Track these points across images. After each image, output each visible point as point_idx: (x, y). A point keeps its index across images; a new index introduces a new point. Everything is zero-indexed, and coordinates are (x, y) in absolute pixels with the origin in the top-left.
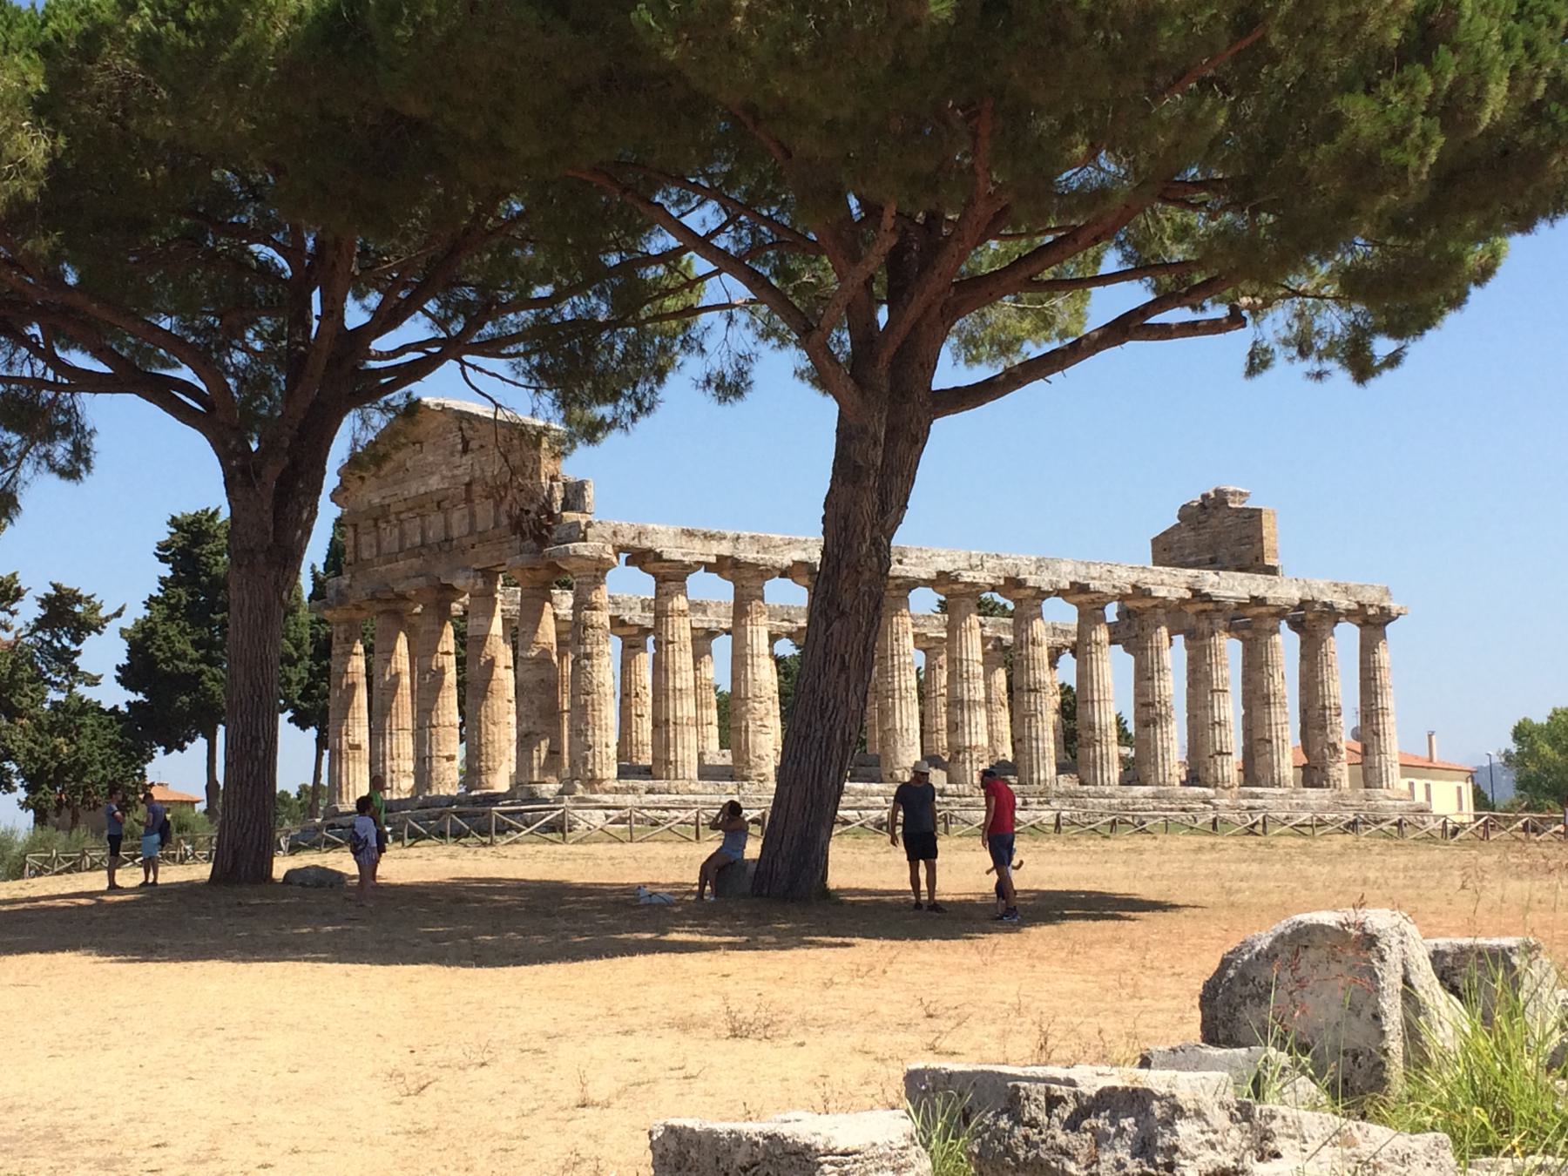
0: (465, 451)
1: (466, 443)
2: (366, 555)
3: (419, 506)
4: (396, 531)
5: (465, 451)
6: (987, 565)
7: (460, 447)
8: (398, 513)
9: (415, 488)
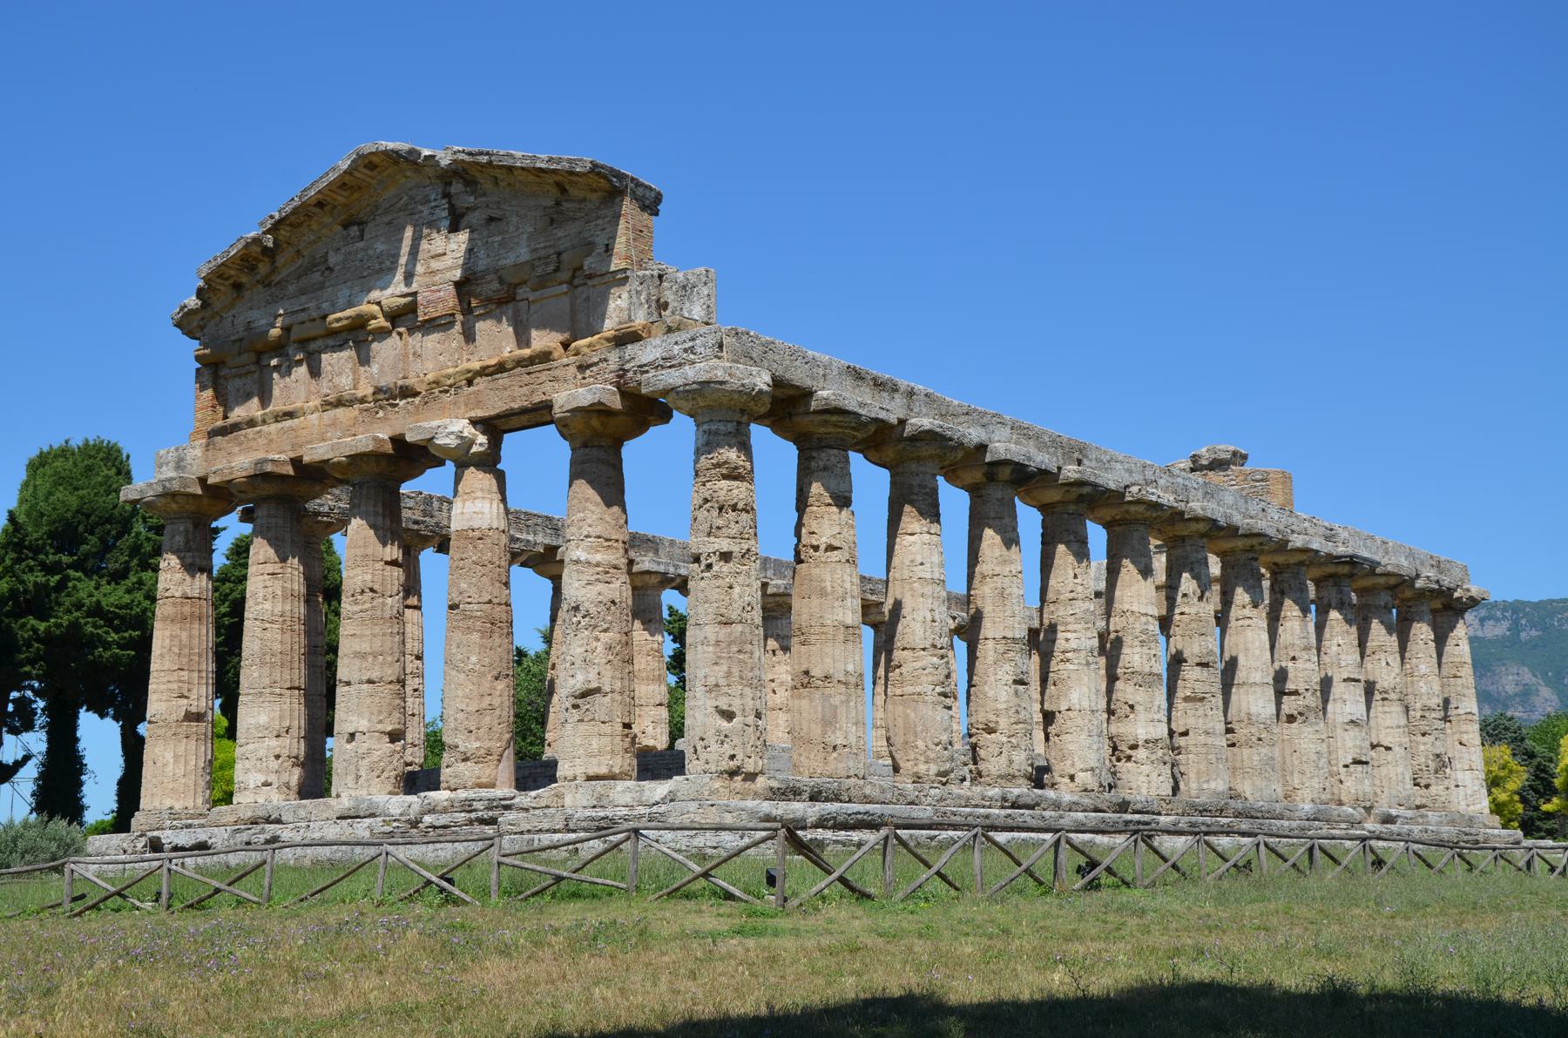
6: (1162, 482)
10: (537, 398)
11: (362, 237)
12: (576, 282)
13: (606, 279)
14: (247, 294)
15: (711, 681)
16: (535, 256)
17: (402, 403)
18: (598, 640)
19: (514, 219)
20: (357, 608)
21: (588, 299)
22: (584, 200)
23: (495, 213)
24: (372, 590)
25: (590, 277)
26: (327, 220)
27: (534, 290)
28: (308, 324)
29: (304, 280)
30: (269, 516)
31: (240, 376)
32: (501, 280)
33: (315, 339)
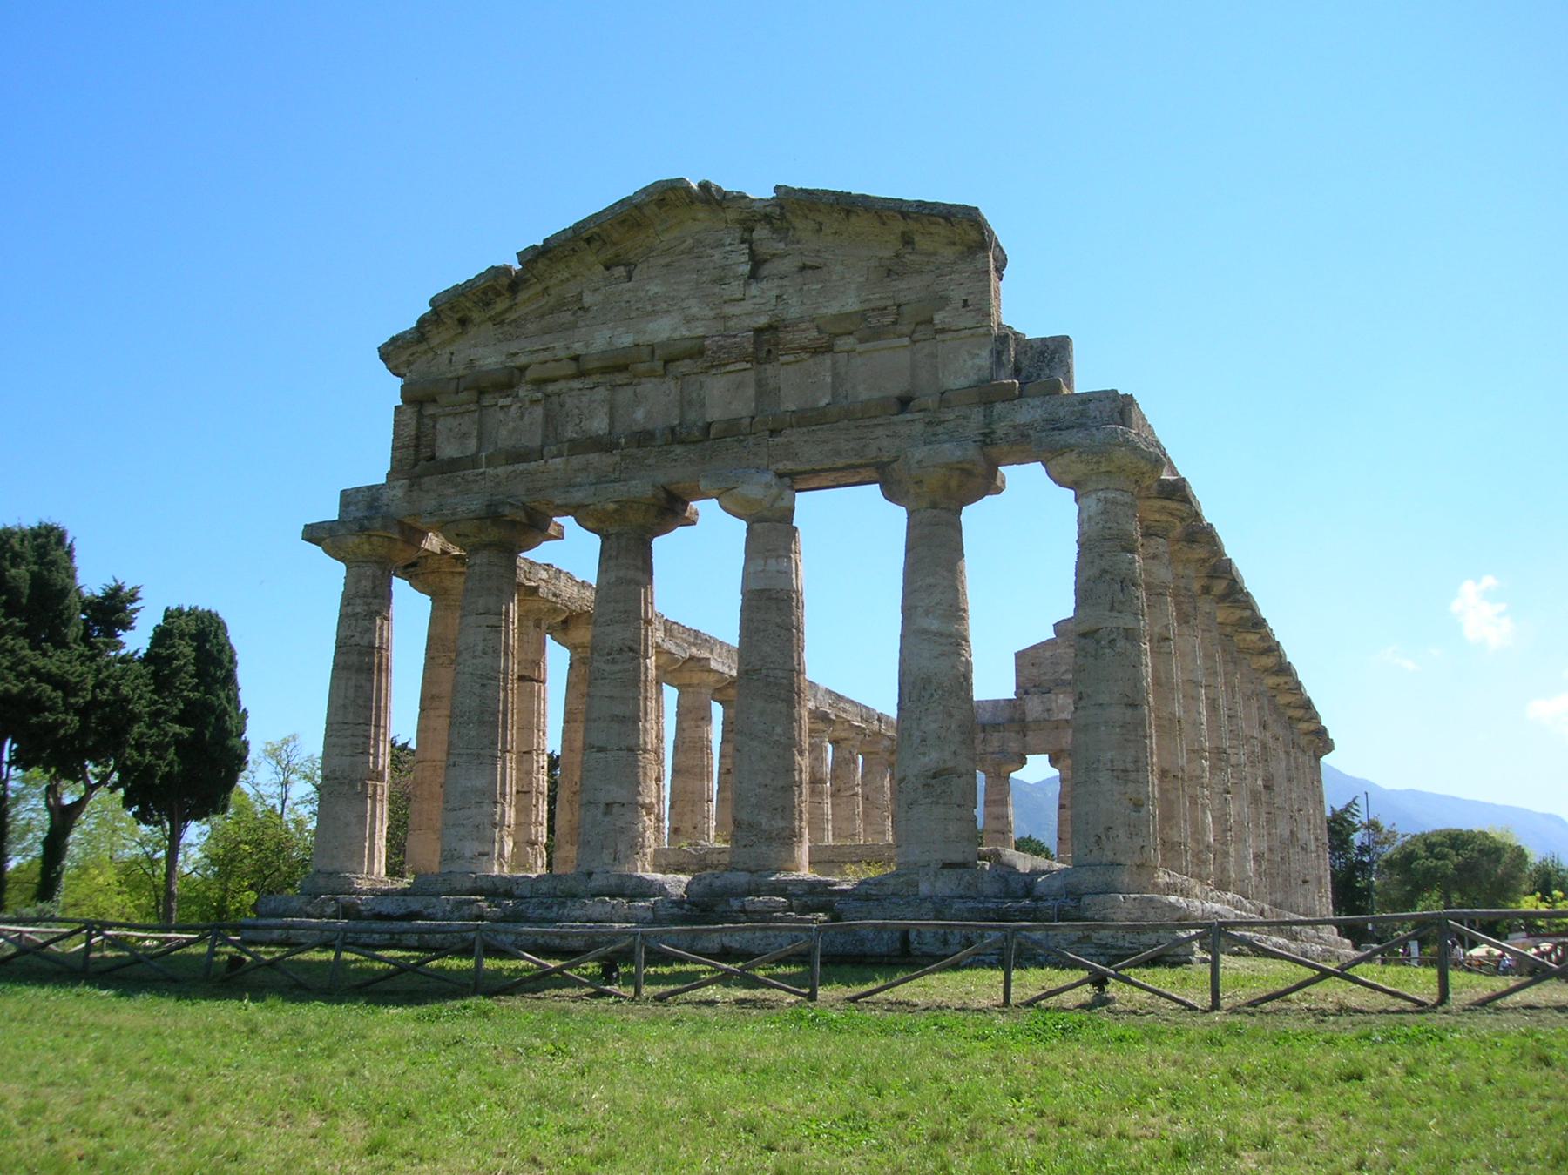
0: (754, 275)
1: (757, 262)
2: (448, 450)
3: (618, 367)
4: (538, 411)
5: (754, 275)
7: (746, 269)
8: (540, 383)
9: (600, 339)
10: (871, 453)
11: (630, 279)
12: (916, 336)
13: (963, 333)
14: (473, 331)
15: (1119, 765)
16: (866, 306)
17: (679, 450)
18: (951, 715)
19: (839, 268)
20: (616, 668)
21: (933, 356)
22: (935, 254)
24: (631, 649)
25: (943, 331)
26: (591, 258)
27: (861, 341)
28: (551, 365)
30: (489, 563)
32: (819, 330)
33: (554, 380)
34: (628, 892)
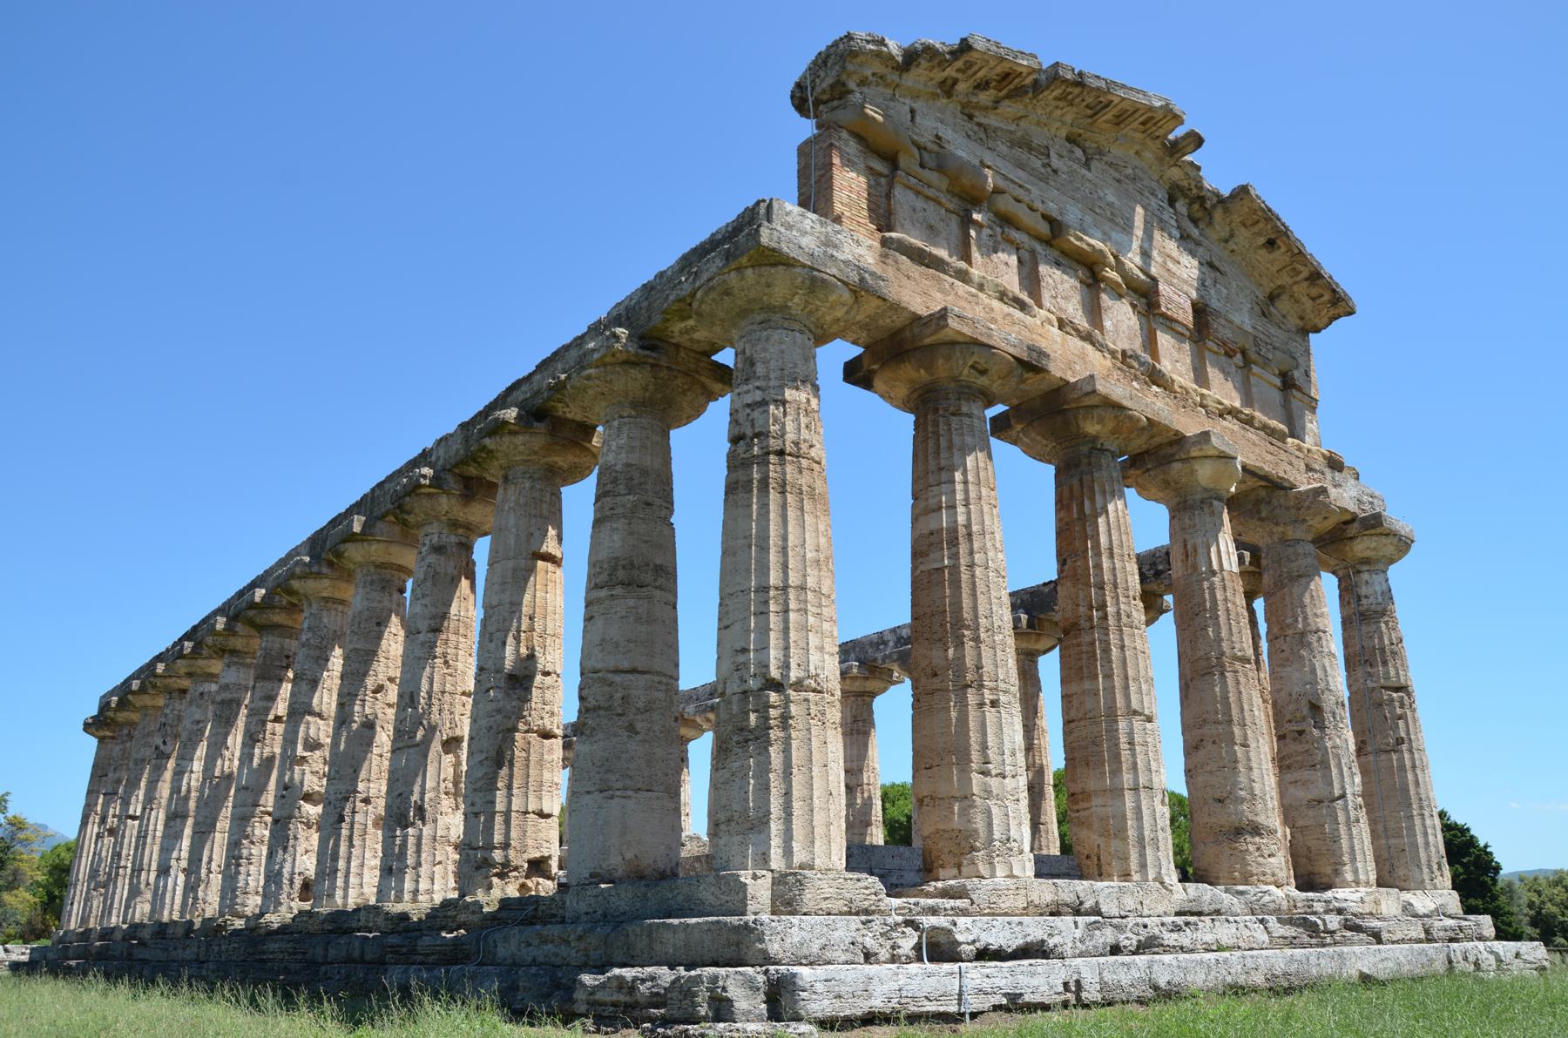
11: (1087, 165)
17: (1155, 388)
23: (1217, 263)
29: (1017, 152)
31: (918, 193)
34: (1206, 909)
